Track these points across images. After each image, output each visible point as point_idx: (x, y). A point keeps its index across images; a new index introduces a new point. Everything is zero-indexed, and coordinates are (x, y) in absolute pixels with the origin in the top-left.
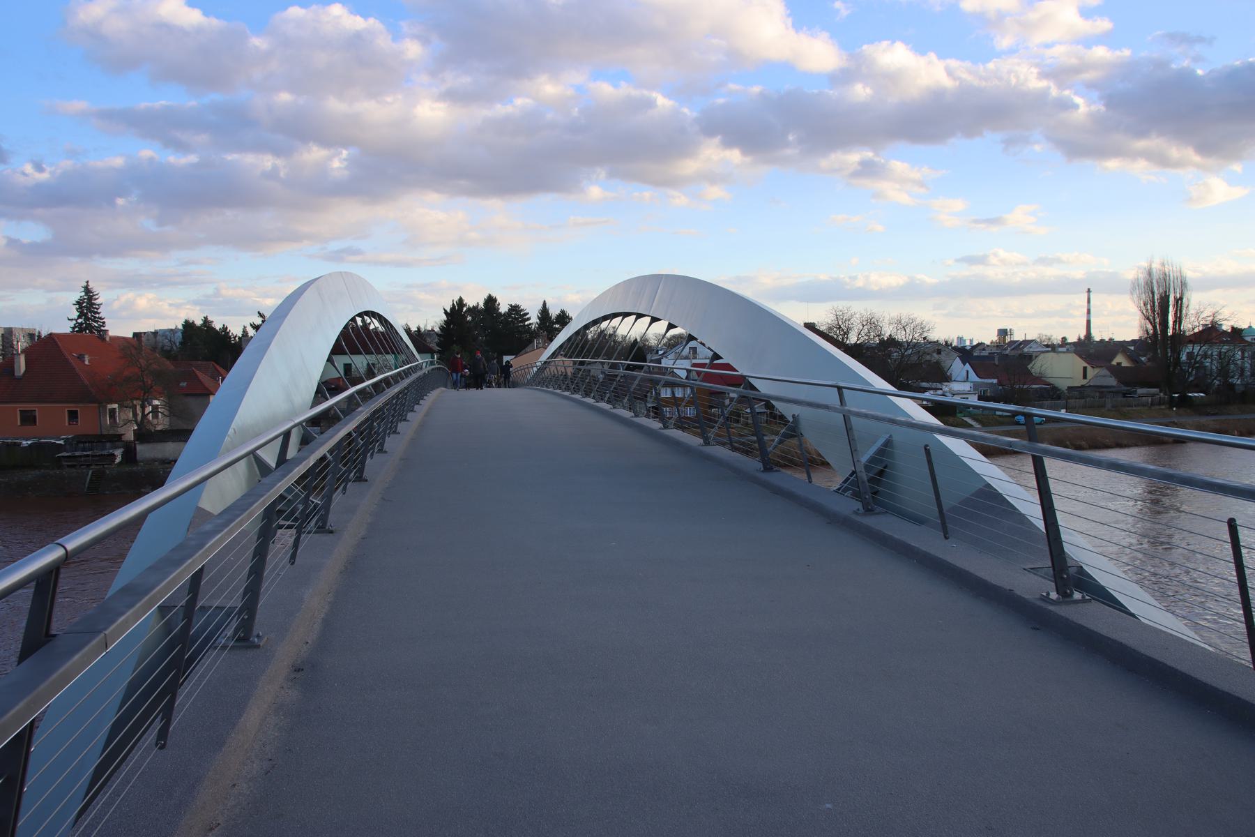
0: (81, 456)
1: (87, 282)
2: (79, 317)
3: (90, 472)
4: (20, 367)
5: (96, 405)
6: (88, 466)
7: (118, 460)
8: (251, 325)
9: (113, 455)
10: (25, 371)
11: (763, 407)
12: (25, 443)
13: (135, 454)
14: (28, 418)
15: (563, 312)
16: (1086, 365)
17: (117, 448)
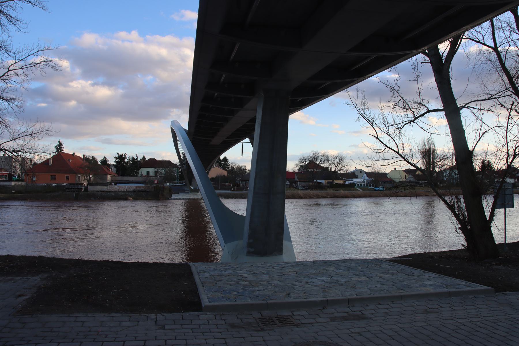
0: (72, 189)
1: (60, 140)
2: (56, 152)
3: (75, 193)
4: (50, 162)
5: (75, 174)
6: (74, 192)
7: (83, 190)
8: (114, 157)
9: (82, 189)
10: (52, 164)
12: (54, 185)
13: (88, 189)
14: (53, 178)
16: (406, 174)
17: (83, 187)
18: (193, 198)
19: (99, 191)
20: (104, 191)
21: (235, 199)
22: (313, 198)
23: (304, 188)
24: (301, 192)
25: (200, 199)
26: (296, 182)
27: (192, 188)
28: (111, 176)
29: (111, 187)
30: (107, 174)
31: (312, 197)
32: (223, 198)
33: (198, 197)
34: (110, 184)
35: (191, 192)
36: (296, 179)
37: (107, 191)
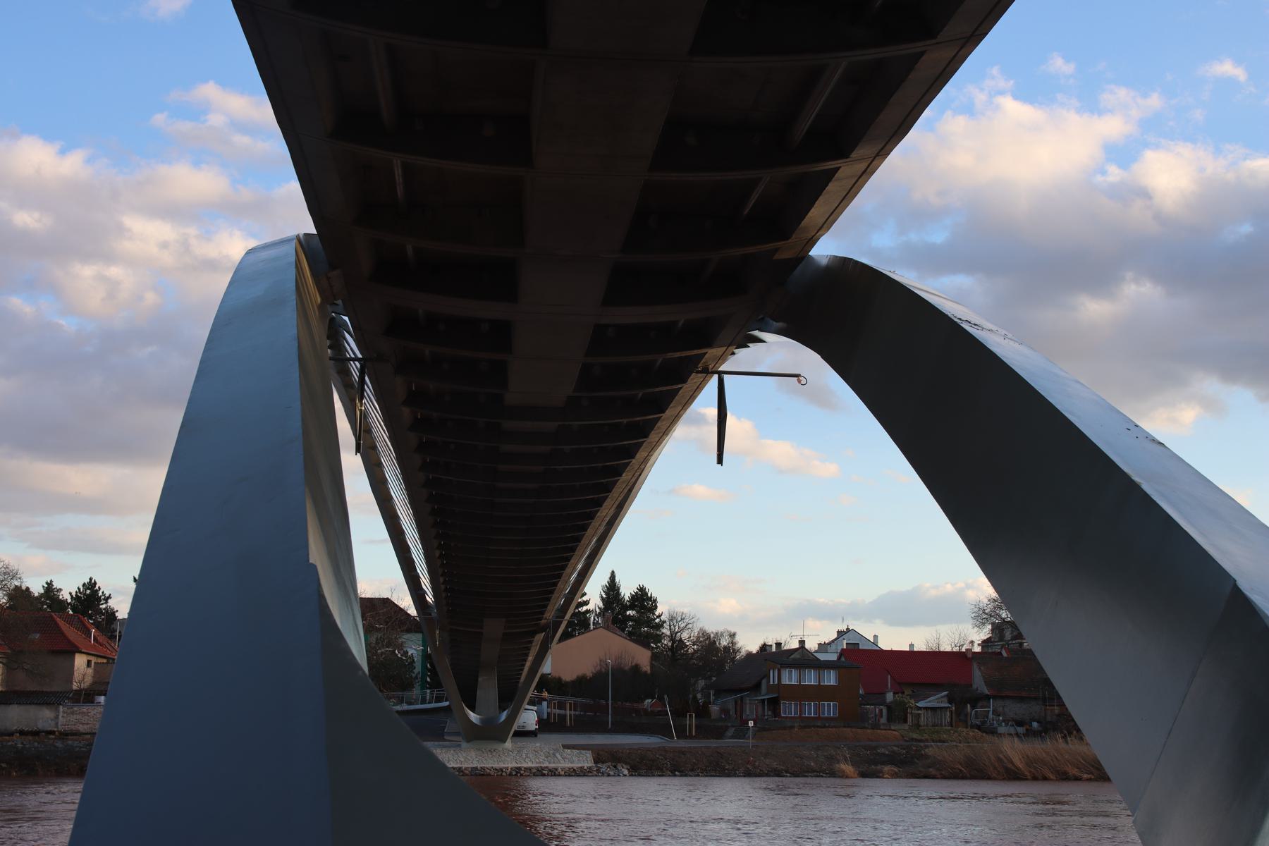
11: (945, 699)
15: (642, 590)
18: (477, 768)
19: (11, 734)
20: (36, 733)
21: (683, 774)
22: (1077, 779)
23: (1021, 730)
24: (1014, 749)
25: (510, 774)
26: (977, 700)
27: (473, 716)
28: (94, 660)
29: (73, 713)
30: (72, 650)
31: (1075, 772)
32: (626, 772)
33: (502, 765)
34: (87, 696)
35: (468, 741)
36: (979, 682)
37: (52, 732)
